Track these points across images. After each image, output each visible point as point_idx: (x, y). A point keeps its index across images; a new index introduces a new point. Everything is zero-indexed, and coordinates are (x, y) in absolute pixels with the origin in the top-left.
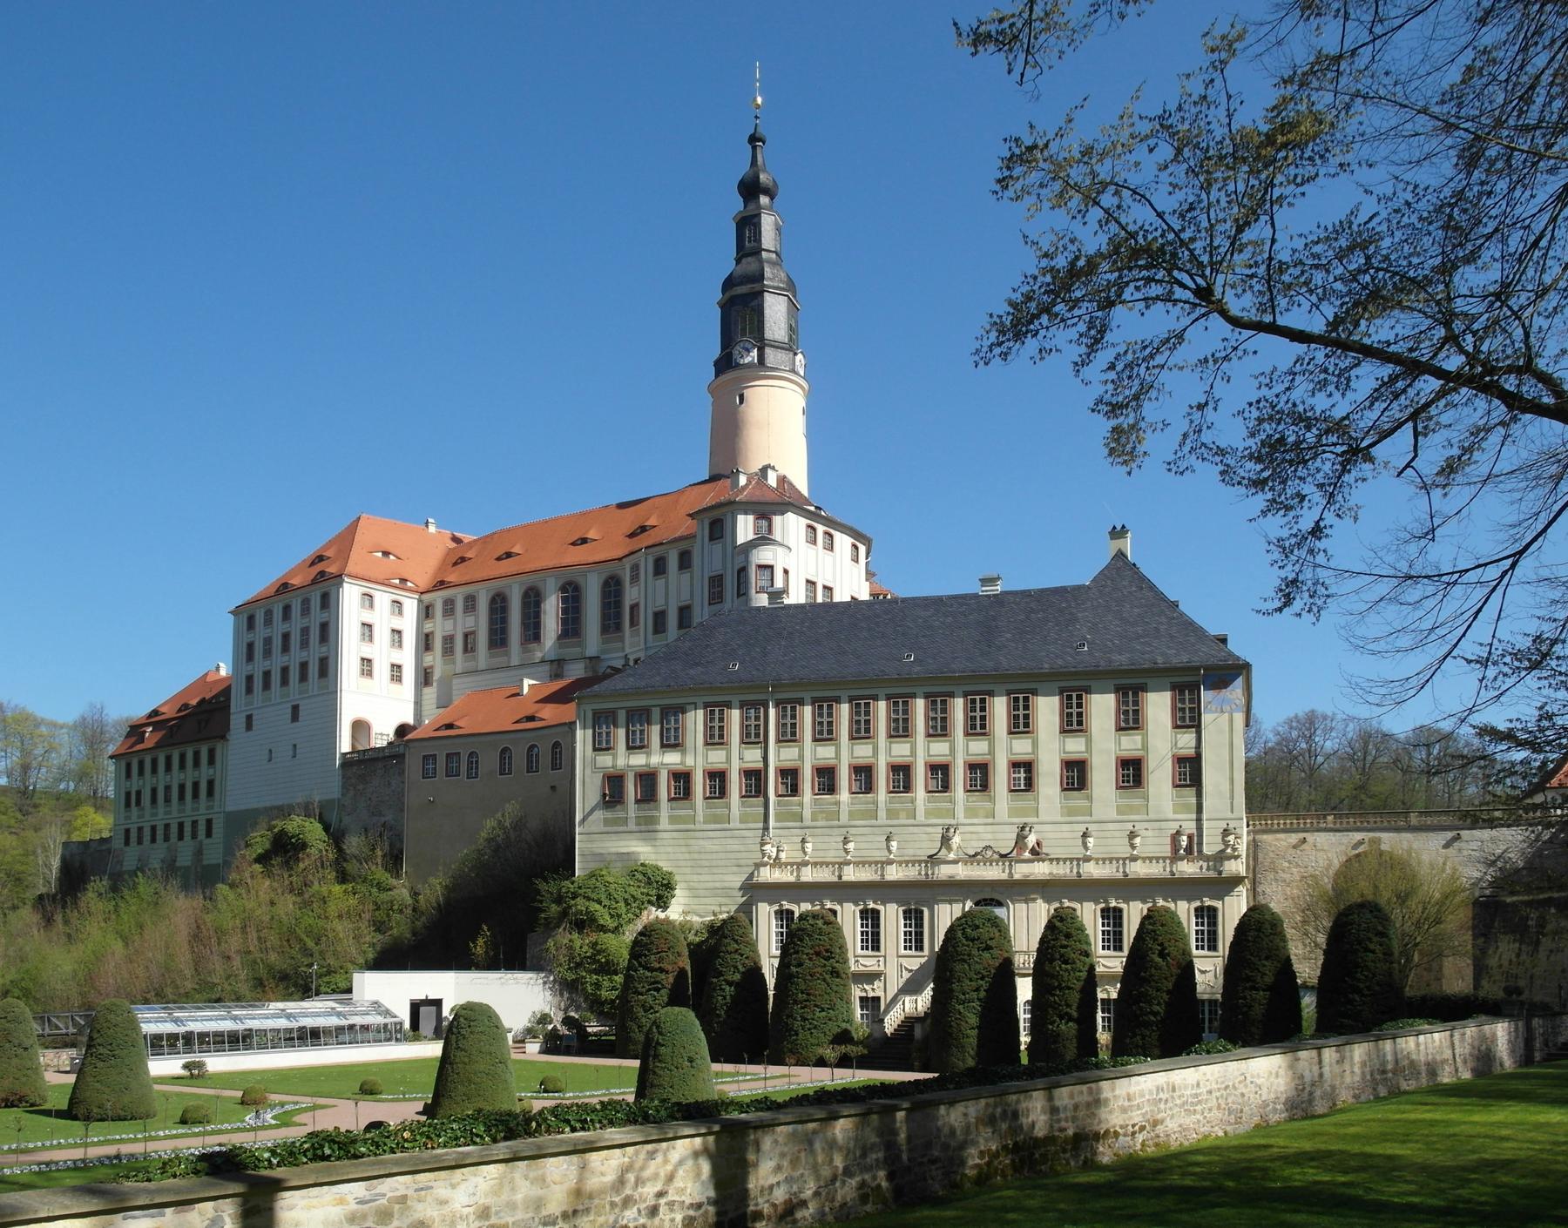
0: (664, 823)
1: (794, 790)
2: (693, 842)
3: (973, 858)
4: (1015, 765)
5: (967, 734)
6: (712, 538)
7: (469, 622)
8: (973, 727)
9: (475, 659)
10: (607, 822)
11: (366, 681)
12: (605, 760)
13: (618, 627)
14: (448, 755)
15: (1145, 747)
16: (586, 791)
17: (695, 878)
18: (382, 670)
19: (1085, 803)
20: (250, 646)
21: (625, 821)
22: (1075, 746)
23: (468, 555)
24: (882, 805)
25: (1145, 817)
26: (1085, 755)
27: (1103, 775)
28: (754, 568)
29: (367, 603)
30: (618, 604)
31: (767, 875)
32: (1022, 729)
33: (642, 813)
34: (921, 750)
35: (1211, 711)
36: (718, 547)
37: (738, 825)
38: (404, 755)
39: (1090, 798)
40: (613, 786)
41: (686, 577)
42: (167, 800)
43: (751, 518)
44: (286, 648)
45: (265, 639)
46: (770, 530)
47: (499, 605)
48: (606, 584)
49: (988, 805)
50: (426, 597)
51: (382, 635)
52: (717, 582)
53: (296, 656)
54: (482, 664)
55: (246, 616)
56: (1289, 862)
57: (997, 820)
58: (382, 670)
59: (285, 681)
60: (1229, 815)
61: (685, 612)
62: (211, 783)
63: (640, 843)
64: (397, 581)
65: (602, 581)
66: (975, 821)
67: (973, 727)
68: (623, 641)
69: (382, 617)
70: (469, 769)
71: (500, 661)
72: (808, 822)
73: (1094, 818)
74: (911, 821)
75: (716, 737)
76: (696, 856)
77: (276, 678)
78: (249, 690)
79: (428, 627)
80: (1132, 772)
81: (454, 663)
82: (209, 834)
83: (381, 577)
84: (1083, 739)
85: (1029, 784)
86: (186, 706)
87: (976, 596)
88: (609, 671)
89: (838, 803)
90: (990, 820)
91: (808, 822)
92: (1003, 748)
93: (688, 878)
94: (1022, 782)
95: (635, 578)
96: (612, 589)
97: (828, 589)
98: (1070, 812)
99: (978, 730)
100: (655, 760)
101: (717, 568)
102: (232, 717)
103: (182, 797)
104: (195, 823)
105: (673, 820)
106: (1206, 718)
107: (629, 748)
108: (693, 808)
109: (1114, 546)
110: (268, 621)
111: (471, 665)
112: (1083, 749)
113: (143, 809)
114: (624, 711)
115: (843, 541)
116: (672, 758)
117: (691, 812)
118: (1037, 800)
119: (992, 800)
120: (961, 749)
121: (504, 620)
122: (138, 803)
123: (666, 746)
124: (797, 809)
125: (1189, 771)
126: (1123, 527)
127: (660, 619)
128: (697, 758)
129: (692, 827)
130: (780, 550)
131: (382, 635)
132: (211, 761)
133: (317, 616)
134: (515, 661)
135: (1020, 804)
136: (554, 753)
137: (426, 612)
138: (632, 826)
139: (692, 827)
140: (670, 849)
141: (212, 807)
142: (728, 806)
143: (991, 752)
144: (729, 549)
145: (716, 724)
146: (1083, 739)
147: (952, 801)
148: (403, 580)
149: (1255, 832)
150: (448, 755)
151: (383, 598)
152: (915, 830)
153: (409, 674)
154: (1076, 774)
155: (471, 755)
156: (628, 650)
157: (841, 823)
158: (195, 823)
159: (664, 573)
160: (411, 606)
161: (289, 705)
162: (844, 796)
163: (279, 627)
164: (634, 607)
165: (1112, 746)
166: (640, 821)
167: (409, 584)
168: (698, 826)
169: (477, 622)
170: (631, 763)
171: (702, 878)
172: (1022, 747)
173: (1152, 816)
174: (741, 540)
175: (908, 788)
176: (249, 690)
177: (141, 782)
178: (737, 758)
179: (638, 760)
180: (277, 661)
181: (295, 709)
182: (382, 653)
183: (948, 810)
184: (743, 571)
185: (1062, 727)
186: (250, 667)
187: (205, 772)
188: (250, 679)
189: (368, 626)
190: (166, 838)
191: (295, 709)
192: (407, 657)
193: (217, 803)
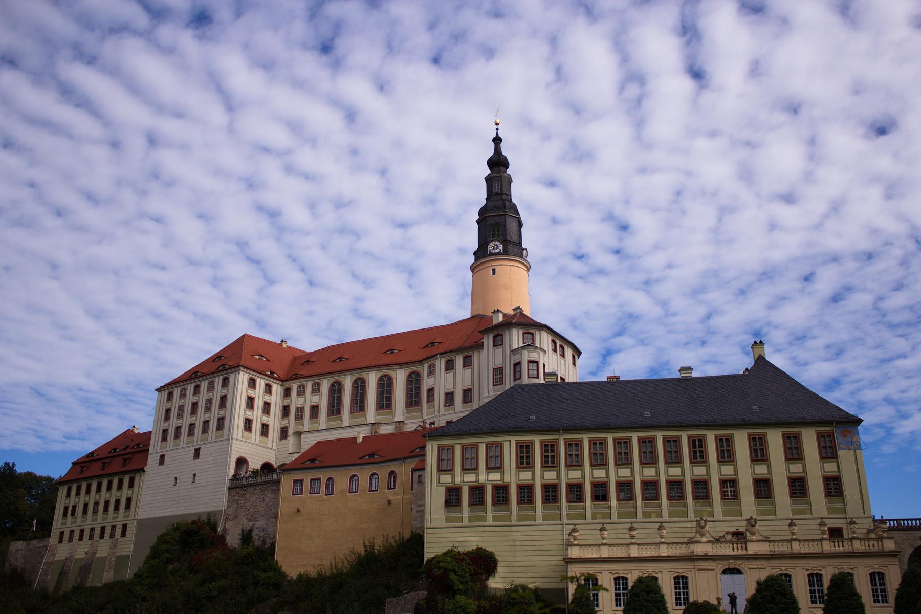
0: (489, 521)
1: (580, 499)
2: (508, 534)
3: (718, 541)
4: (723, 482)
5: (691, 462)
6: (494, 346)
7: (315, 399)
8: (695, 458)
9: (318, 422)
10: (447, 520)
11: (247, 434)
12: (446, 479)
14: (312, 480)
16: (435, 497)
17: (511, 559)
18: (256, 428)
20: (168, 411)
21: (461, 519)
23: (312, 359)
24: (639, 509)
25: (810, 516)
26: (768, 476)
27: (781, 489)
28: (526, 362)
29: (251, 385)
30: (418, 388)
31: (575, 553)
32: (726, 459)
34: (664, 473)
35: (842, 449)
36: (499, 351)
37: (542, 522)
38: (278, 482)
39: (774, 504)
40: (453, 497)
41: (468, 371)
42: (95, 512)
44: (194, 411)
45: (179, 407)
46: (533, 343)
47: (336, 391)
49: (709, 508)
50: (287, 384)
51: (258, 405)
52: (498, 373)
53: (201, 416)
54: (323, 426)
55: (167, 392)
57: (716, 518)
58: (256, 428)
59: (191, 433)
60: (865, 516)
61: (467, 395)
62: (129, 500)
63: (473, 534)
64: (269, 373)
65: (406, 375)
67: (695, 458)
68: (421, 411)
69: (259, 394)
71: (336, 423)
72: (589, 520)
73: (778, 517)
75: (524, 461)
76: (512, 543)
77: (185, 431)
78: (165, 438)
79: (287, 402)
80: (798, 487)
81: (303, 425)
82: (124, 534)
83: (260, 370)
84: (766, 466)
85: (735, 496)
86: (115, 450)
87: (678, 379)
88: (419, 428)
89: (610, 507)
92: (716, 472)
93: (507, 559)
94: (729, 494)
95: (431, 372)
96: (414, 382)
97: (562, 378)
98: (762, 513)
99: (699, 459)
100: (482, 478)
101: (499, 363)
102: (149, 457)
103: (106, 509)
104: (114, 527)
105: (495, 518)
106: (841, 453)
108: (509, 510)
109: (758, 351)
110: (183, 395)
111: (314, 426)
112: (766, 472)
113: (76, 518)
114: (460, 446)
115: (569, 352)
116: (495, 477)
117: (507, 513)
118: (740, 505)
119: (711, 505)
120: (689, 472)
121: (340, 398)
122: (73, 514)
123: (489, 469)
124: (582, 511)
125: (833, 487)
126: (761, 342)
127: (449, 397)
128: (512, 476)
129: (508, 523)
130: (541, 353)
131: (258, 405)
132: (131, 485)
133: (219, 391)
134: (345, 424)
135: (728, 508)
136: (389, 479)
137: (287, 393)
138: (466, 522)
139: (508, 523)
140: (493, 539)
141: (129, 516)
142: (534, 509)
144: (507, 352)
145: (525, 455)
146: (766, 466)
147: (686, 506)
148: (272, 373)
150: (312, 480)
151: (261, 383)
153: (274, 431)
154: (763, 488)
155: (330, 479)
157: (612, 521)
158: (114, 527)
159: (453, 369)
160: (277, 388)
161: (193, 448)
162: (614, 502)
163: (190, 398)
164: (431, 391)
166: (471, 519)
167: (275, 375)
168: (513, 523)
169: (320, 399)
170: (465, 480)
171: (517, 559)
172: (728, 470)
175: (657, 497)
176: (165, 438)
177: (77, 500)
178: (539, 476)
179: (470, 478)
180: (187, 419)
181: (197, 451)
182: (257, 416)
183: (683, 512)
184: (517, 365)
186: (167, 424)
187: (126, 492)
188: (165, 432)
189: (250, 401)
190: (91, 538)
191: (197, 451)
192: (274, 421)
193: (132, 513)
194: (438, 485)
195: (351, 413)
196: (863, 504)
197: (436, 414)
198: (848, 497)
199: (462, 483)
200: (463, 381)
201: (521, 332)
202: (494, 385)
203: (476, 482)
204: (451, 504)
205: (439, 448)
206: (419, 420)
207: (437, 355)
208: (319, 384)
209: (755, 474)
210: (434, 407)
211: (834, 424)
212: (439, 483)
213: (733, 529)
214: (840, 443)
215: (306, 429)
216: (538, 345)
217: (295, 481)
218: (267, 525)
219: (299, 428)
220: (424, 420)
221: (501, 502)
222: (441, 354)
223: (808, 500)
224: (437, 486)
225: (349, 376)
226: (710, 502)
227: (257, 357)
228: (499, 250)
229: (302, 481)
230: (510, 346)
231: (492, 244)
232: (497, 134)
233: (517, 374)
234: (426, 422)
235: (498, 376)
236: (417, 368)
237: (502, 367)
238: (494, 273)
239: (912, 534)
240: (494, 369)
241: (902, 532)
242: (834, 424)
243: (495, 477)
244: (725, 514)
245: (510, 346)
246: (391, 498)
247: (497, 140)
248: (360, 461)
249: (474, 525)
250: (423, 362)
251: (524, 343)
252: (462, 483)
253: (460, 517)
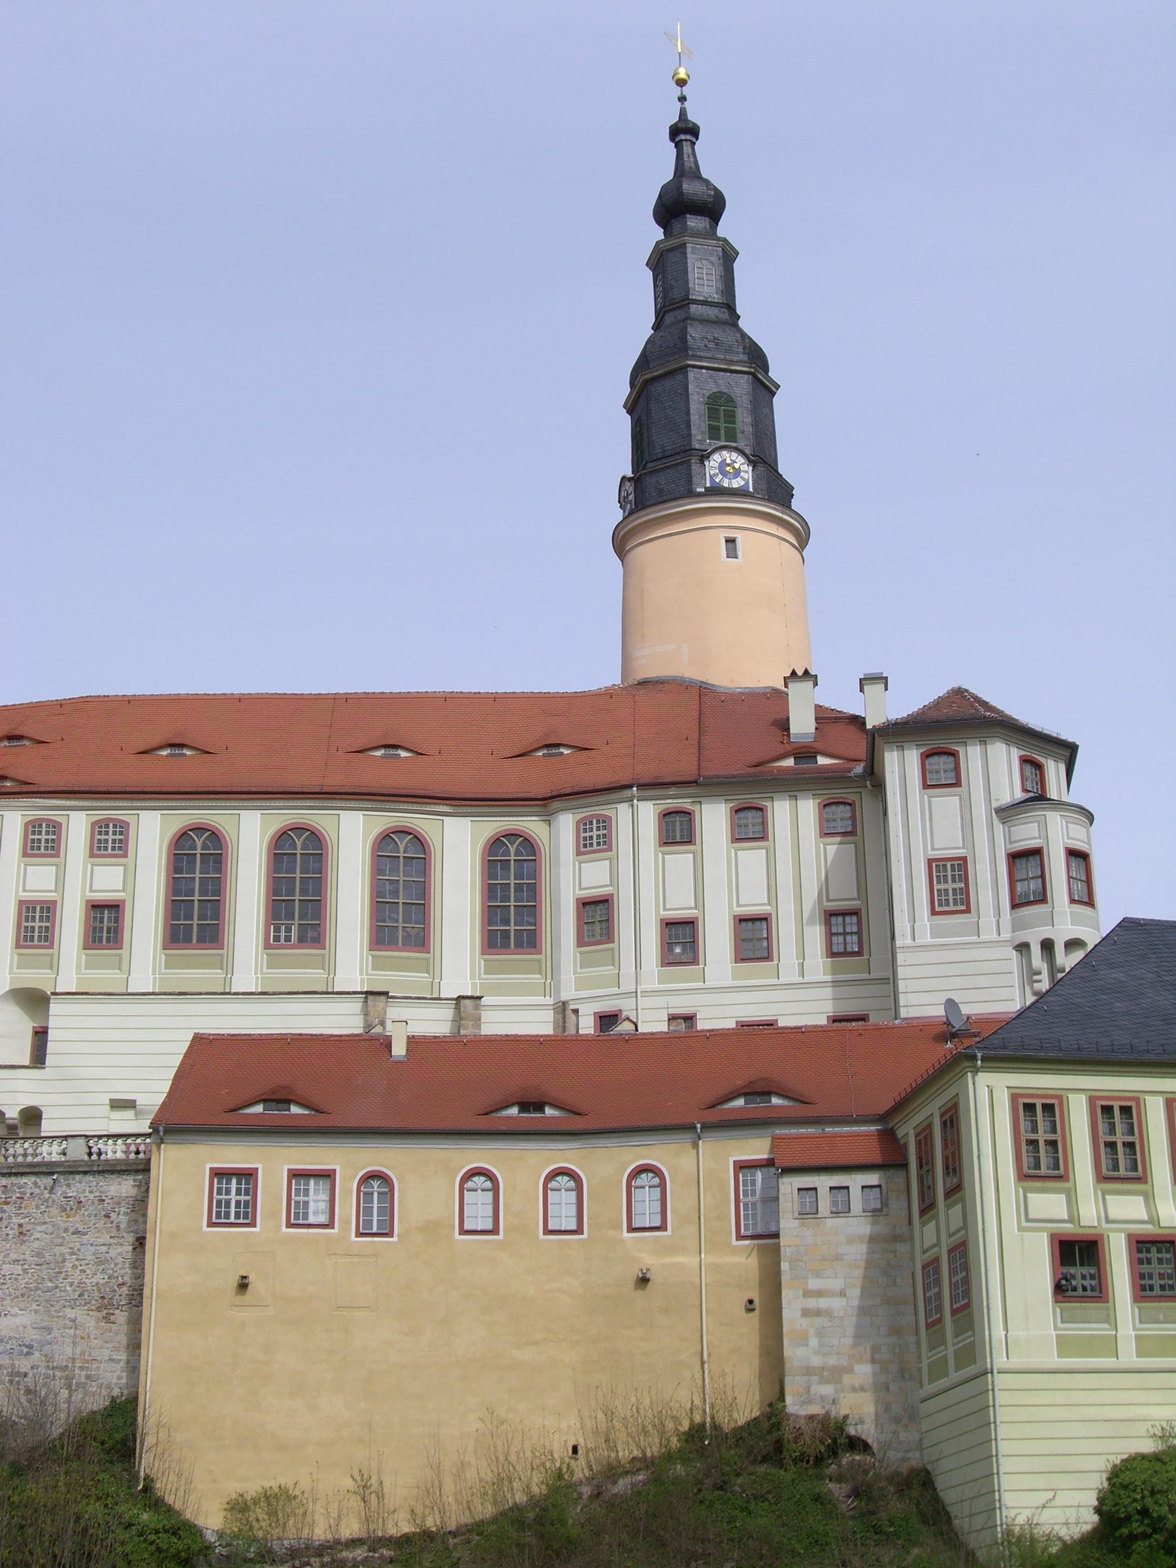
10: (1065, 1345)
13: (530, 941)
14: (295, 1175)
21: (1111, 1346)
30: (531, 890)
33: (1152, 1330)
41: (752, 858)
48: (496, 844)
70: (363, 1211)
81: (53, 965)
101: (949, 843)
107: (1101, 1178)
111: (106, 977)
138: (1128, 1356)
144: (981, 812)
156: (568, 993)
166: (1144, 1346)
170: (1114, 1213)
194: (1024, 1224)
195: (267, 946)
197: (628, 985)
199: (1104, 1225)
200: (734, 886)
201: (913, 756)
202: (934, 912)
203: (1151, 1221)
204: (1080, 1292)
205: (1014, 1098)
206: (539, 1000)
207: (630, 787)
208: (605, 823)
210: (614, 961)
212: (1028, 1220)
215: (68, 981)
217: (219, 1174)
218: (49, 1330)
219: (37, 978)
220: (564, 1004)
221: (1157, 1291)
222: (642, 786)
224: (1021, 1229)
225: (82, 814)
228: (742, 483)
229: (248, 1176)
230: (988, 792)
231: (717, 458)
233: (1019, 887)
234: (576, 1011)
235: (950, 886)
236: (532, 825)
237: (964, 859)
238: (732, 552)
240: (930, 862)
245: (988, 792)
246: (649, 1260)
248: (483, 1123)
249: (1091, 1366)
250: (556, 804)
251: (1025, 790)
252: (1104, 1225)
253: (1111, 1335)
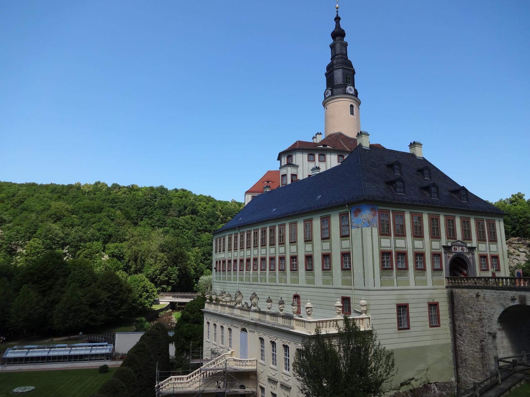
15: (331, 249)
19: (311, 277)
22: (309, 247)
39: (314, 275)
43: (286, 158)
46: (292, 162)
56: (471, 307)
60: (363, 287)
66: (282, 284)
73: (315, 286)
74: (265, 283)
90: (285, 284)
91: (244, 282)
119: (286, 275)
143: (285, 252)
147: (275, 275)
149: (451, 287)
152: (267, 287)
165: (320, 248)
173: (334, 286)
174: (283, 164)
185: (304, 239)
196: (364, 277)
198: (355, 271)
209: (306, 252)
211: (347, 206)
213: (294, 293)
214: (353, 222)
216: (294, 163)
223: (331, 272)
226: (285, 272)
227: (266, 183)
232: (337, 14)
239: (504, 293)
241: (494, 291)
242: (347, 206)
243: (223, 256)
244: (293, 281)
247: (337, 19)
